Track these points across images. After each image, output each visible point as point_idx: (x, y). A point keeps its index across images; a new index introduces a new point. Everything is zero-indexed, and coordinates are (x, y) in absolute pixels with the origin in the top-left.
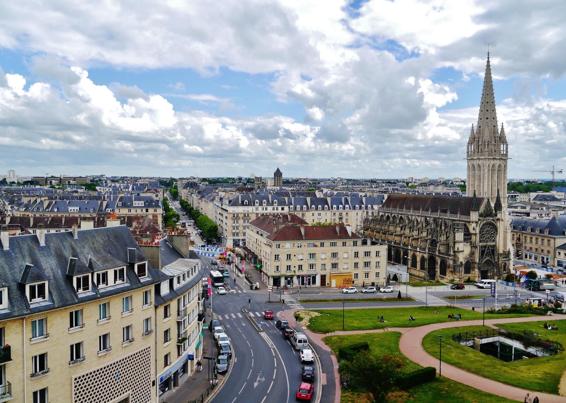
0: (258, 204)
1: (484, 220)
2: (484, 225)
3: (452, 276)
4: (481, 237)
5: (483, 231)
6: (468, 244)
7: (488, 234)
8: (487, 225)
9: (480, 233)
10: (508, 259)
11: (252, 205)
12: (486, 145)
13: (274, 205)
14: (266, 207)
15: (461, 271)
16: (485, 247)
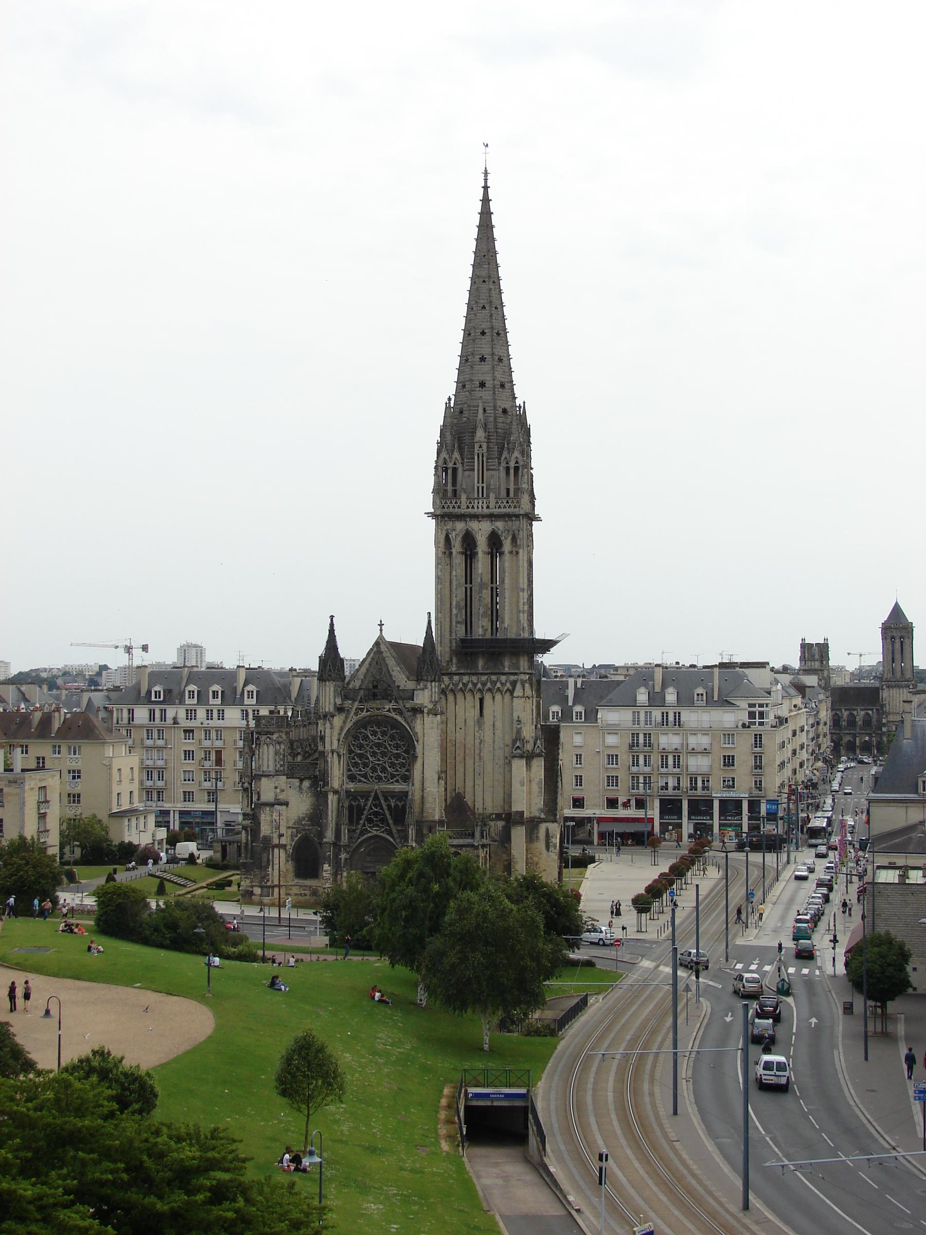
0: (195, 701)
1: (362, 710)
2: (362, 724)
3: (248, 881)
4: (356, 765)
5: (361, 747)
6: (306, 784)
7: (384, 754)
8: (379, 724)
9: (350, 752)
10: (469, 841)
11: (177, 701)
12: (512, 471)
13: (247, 701)
14: (222, 707)
15: (263, 865)
16: (365, 795)
